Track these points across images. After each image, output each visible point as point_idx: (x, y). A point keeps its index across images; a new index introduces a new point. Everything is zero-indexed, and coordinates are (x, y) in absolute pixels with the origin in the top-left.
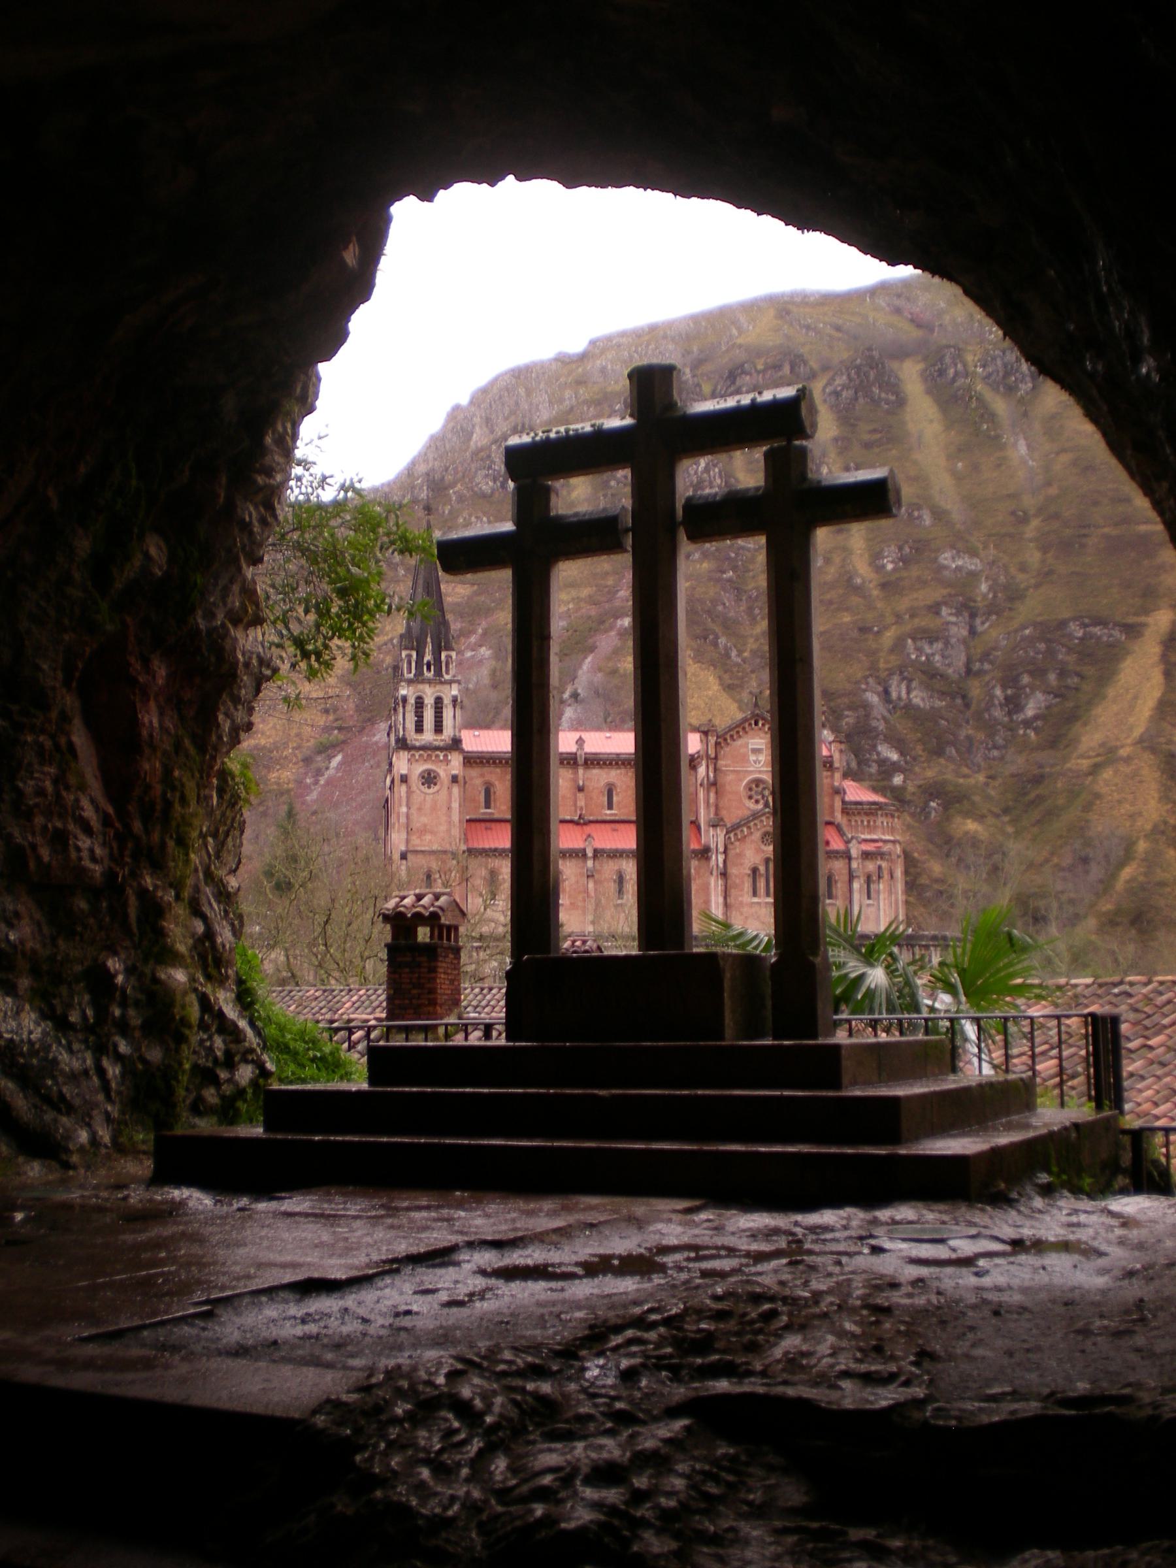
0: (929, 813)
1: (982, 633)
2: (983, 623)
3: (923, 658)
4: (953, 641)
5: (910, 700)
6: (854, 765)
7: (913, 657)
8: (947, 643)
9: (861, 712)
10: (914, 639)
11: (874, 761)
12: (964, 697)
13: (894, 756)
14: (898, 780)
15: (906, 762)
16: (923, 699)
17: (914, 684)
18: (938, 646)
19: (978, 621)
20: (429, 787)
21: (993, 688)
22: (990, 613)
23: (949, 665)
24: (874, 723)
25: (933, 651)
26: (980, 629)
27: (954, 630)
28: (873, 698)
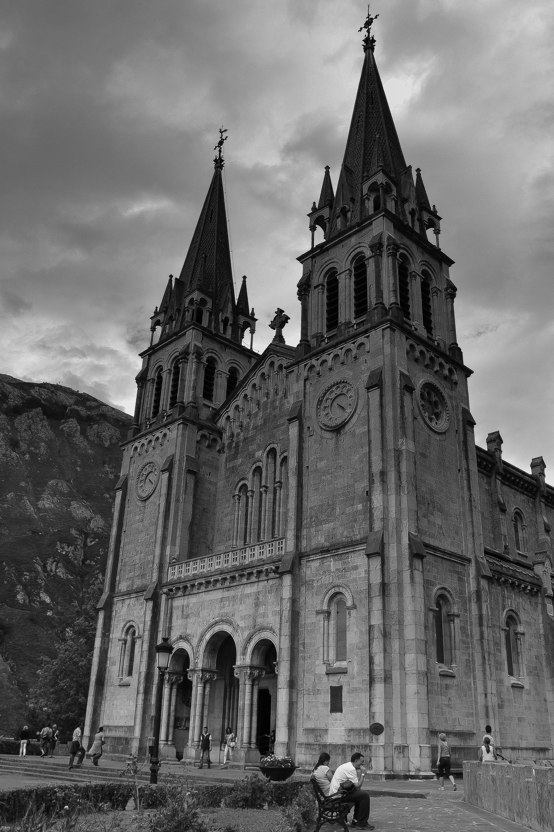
0: (65, 634)
1: (90, 546)
2: (91, 542)
3: (64, 553)
4: (79, 547)
5: (56, 573)
6: (27, 601)
7: (59, 551)
8: (76, 547)
9: (33, 574)
10: (61, 543)
11: (38, 601)
12: (81, 577)
13: (48, 600)
14: (49, 613)
15: (53, 604)
16: (63, 573)
17: (60, 565)
18: (71, 548)
19: (89, 540)
20: (431, 419)
21: (97, 574)
22: (95, 538)
23: (76, 559)
24: (40, 581)
25: (68, 550)
26: (89, 544)
27: (79, 542)
28: (40, 569)
